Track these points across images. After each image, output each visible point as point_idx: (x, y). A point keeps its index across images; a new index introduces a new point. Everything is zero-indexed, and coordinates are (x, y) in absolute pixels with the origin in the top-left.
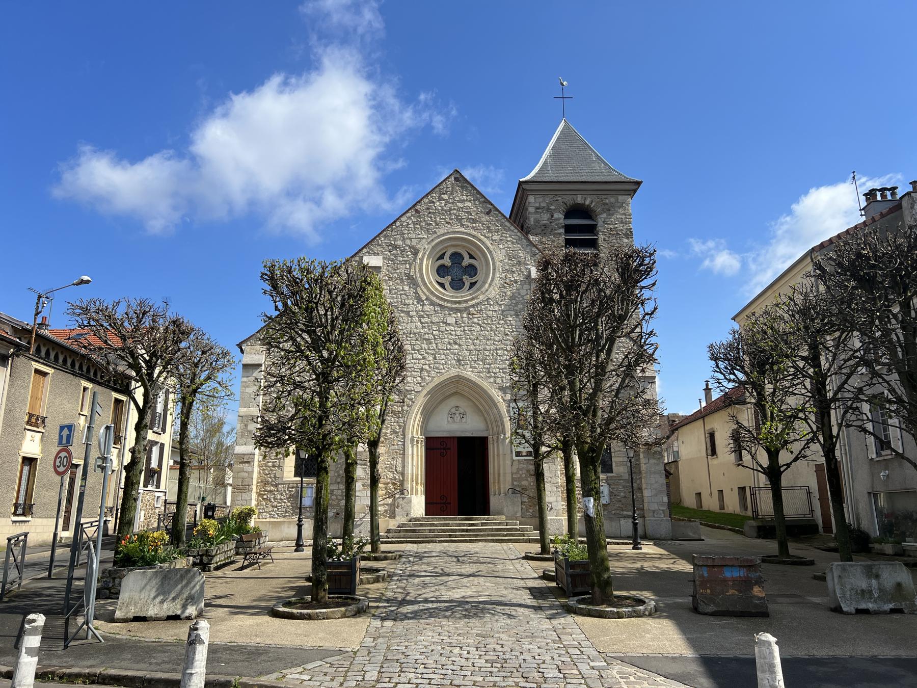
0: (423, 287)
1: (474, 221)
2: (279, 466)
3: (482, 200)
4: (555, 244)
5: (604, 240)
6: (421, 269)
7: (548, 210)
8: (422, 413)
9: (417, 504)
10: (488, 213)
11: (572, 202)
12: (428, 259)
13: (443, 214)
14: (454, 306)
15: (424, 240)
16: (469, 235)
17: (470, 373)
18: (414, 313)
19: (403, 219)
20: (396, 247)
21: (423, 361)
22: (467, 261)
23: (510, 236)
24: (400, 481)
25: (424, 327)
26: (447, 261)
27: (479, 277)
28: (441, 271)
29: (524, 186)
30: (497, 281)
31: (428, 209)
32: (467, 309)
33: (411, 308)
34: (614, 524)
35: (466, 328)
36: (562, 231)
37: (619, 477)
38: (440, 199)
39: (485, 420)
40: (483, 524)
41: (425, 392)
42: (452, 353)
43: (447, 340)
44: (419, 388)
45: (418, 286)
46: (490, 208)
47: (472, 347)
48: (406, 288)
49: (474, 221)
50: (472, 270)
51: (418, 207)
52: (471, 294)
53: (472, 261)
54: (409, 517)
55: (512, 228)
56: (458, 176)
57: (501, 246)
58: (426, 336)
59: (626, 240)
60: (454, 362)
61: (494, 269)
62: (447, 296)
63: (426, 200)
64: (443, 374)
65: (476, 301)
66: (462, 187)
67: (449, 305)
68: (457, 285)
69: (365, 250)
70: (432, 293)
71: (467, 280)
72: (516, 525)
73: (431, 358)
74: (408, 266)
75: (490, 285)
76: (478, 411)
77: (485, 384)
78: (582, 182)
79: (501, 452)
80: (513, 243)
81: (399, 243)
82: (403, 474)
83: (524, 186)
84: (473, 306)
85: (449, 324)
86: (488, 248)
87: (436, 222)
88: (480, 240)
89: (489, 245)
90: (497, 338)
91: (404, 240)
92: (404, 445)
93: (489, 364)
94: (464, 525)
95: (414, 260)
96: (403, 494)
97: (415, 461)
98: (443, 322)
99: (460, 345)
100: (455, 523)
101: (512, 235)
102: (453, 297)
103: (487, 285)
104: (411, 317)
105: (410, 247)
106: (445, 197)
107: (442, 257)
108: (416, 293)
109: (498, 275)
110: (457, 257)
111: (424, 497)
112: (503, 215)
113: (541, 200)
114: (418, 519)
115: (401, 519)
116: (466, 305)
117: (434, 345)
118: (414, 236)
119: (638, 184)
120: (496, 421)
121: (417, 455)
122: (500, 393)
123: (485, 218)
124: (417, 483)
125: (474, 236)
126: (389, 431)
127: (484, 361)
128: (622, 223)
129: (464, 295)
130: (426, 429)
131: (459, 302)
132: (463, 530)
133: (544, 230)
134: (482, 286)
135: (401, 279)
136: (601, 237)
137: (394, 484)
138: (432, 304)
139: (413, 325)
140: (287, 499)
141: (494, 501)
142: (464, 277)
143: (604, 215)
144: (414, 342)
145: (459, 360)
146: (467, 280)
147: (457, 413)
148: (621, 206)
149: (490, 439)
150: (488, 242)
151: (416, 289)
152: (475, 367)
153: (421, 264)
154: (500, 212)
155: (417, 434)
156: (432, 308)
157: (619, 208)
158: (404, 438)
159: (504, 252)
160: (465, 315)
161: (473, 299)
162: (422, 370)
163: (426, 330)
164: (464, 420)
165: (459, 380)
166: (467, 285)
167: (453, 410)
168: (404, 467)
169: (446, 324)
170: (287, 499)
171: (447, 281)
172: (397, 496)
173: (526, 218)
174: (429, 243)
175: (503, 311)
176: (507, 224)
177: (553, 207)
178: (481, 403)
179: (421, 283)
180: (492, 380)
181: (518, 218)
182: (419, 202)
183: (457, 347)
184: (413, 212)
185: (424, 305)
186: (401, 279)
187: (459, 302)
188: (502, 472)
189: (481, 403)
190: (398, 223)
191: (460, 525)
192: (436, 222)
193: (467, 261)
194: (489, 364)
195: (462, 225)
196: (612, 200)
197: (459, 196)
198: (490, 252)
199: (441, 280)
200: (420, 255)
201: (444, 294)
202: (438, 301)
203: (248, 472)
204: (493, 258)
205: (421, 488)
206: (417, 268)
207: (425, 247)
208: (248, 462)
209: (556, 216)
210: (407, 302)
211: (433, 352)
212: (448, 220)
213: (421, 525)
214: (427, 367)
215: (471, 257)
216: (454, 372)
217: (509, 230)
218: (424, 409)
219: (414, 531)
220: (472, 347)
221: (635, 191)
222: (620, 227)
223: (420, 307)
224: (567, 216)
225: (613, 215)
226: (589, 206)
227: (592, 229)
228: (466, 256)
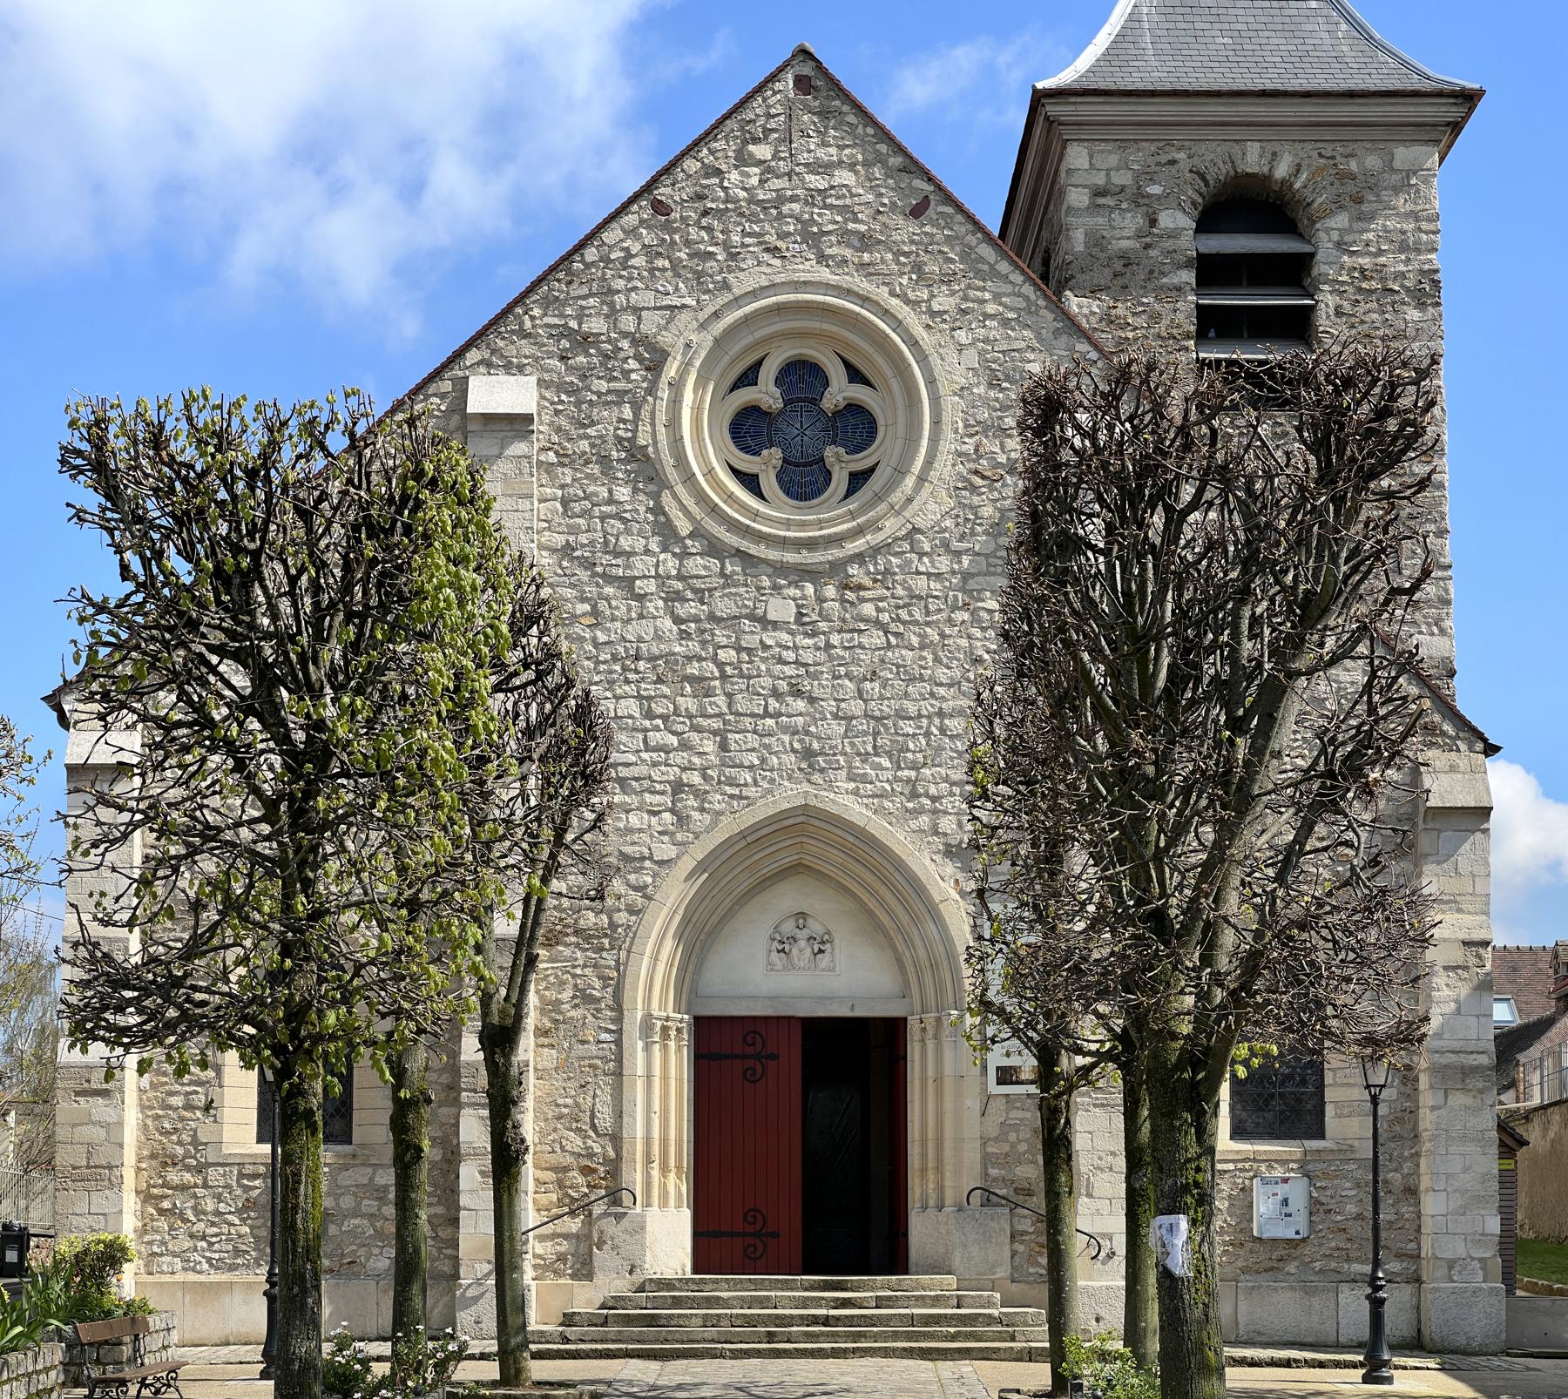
0: (680, 489)
1: (865, 242)
2: (208, 1107)
3: (896, 161)
4: (1162, 327)
5: (1339, 312)
6: (674, 424)
7: (1139, 199)
8: (679, 936)
9: (666, 1237)
10: (917, 212)
12: (701, 383)
13: (753, 218)
14: (791, 557)
15: (685, 316)
16: (848, 293)
17: (849, 800)
18: (650, 586)
19: (609, 237)
20: (585, 341)
21: (681, 758)
22: (839, 391)
23: (997, 297)
24: (606, 1161)
25: (684, 635)
26: (766, 393)
27: (882, 450)
28: (748, 429)
29: (1052, 109)
30: (945, 467)
31: (700, 197)
32: (837, 567)
33: (641, 565)
34: (1316, 1302)
35: (835, 639)
36: (1188, 276)
37: (1344, 1153)
38: (743, 160)
39: (899, 961)
40: (880, 1302)
41: (687, 864)
42: (785, 729)
43: (767, 682)
44: (665, 850)
45: (665, 484)
46: (927, 196)
47: (856, 707)
48: (623, 493)
49: (865, 242)
50: (857, 426)
51: (663, 192)
52: (853, 515)
53: (859, 393)
54: (638, 1278)
55: (1004, 267)
56: (807, 69)
57: (963, 336)
58: (693, 669)
59: (1413, 314)
60: (790, 760)
61: (936, 423)
62: (769, 520)
63: (691, 165)
64: (751, 802)
65: (871, 539)
66: (824, 114)
67: (773, 555)
68: (804, 481)
69: (473, 356)
70: (714, 510)
71: (840, 462)
72: (990, 1304)
73: (709, 746)
74: (627, 413)
75: (922, 479)
76: (875, 928)
77: (899, 839)
78: (1263, 93)
79: (948, 1070)
80: (1005, 323)
81: (596, 325)
82: (616, 1139)
83: (1052, 109)
84: (859, 558)
85: (775, 625)
86: (914, 344)
87: (727, 245)
88: (886, 314)
89: (919, 332)
90: (942, 674)
91: (613, 314)
92: (618, 1043)
93: (915, 767)
94: (817, 1303)
95: (652, 391)
96: (617, 1202)
97: (659, 1098)
98: (752, 617)
99: (812, 700)
100: (791, 1295)
101: (1007, 290)
102: (788, 524)
103: (910, 481)
104: (641, 598)
105: (635, 342)
106: (762, 151)
107: (748, 377)
108: (658, 510)
109: (948, 444)
110: (802, 377)
111: (686, 1215)
112: (970, 218)
113: (1113, 160)
114: (667, 1284)
115: (610, 1283)
116: (835, 553)
117: (721, 701)
118: (647, 299)
119: (1469, 98)
120: (934, 966)
121: (665, 1078)
122: (950, 868)
123: (905, 230)
124: (664, 1169)
125: (864, 300)
126: (567, 995)
127: (897, 755)
128: (1404, 247)
129: (829, 516)
130: (694, 990)
131: (811, 544)
132: (815, 1320)
133: (1123, 274)
134: (891, 486)
135: (604, 461)
136: (1327, 300)
137: (587, 1171)
138: (715, 549)
139: (645, 629)
140: (238, 1211)
141: (921, 1230)
142: (830, 452)
143: (1340, 220)
144: (648, 689)
145: (808, 754)
146: (840, 462)
148: (1402, 187)
149: (913, 1026)
150: (914, 322)
151: (656, 496)
152: (864, 779)
153: (676, 402)
154: (959, 208)
155: (663, 1005)
156: (714, 564)
157: (1397, 190)
158: (619, 1020)
159: (971, 357)
160: (830, 591)
161: (859, 532)
162: (678, 787)
163: (694, 646)
164: (824, 960)
165: (804, 823)
166: (840, 480)
167: (789, 927)
168: (619, 1115)
169: (765, 623)
170: (238, 1211)
171: (767, 464)
172: (598, 1210)
173: (1060, 230)
174: (703, 326)
175: (966, 576)
176: (986, 251)
177: (1155, 190)
178: (882, 903)
179: (672, 475)
180: (924, 821)
181: (1032, 234)
182: (667, 170)
183: (801, 705)
184: (643, 210)
185: (685, 554)
186: (604, 461)
187: (811, 544)
188: (948, 1133)
189: (882, 903)
190: (591, 254)
191: (805, 1303)
192: (727, 245)
193: (839, 391)
194: (915, 767)
195: (822, 258)
196: (1373, 162)
197: (812, 148)
198: (923, 359)
199: (747, 463)
200: (671, 370)
201: (756, 515)
202: (733, 540)
203: (106, 1126)
204: (931, 382)
205: (679, 1186)
206: (662, 418)
207: (689, 340)
208: (104, 1093)
209: (1167, 220)
210: (625, 543)
211: (716, 724)
212: (772, 239)
213: (677, 1302)
214: (696, 778)
215: (855, 375)
216: (789, 795)
217: (994, 274)
218: (686, 921)
219: (652, 1321)
220: (856, 707)
221: (1456, 127)
222: (1394, 263)
223: (670, 564)
224: (1207, 222)
225: (1372, 218)
226: (1286, 184)
227: (1295, 271)
228: (837, 374)
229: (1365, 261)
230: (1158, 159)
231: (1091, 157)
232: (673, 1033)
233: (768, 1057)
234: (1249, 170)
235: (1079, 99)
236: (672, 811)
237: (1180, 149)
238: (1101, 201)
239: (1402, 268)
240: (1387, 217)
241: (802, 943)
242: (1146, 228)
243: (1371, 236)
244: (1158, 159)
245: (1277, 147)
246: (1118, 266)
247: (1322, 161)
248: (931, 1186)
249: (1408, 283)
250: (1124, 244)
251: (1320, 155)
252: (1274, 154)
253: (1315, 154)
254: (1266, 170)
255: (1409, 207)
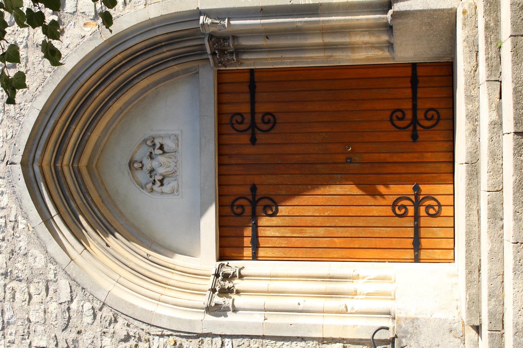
114: (474, 303)
147: (148, 164)
164: (169, 144)
232: (227, 284)
233: (254, 196)
236: (29, 281)
241: (155, 164)
248: (367, 39)
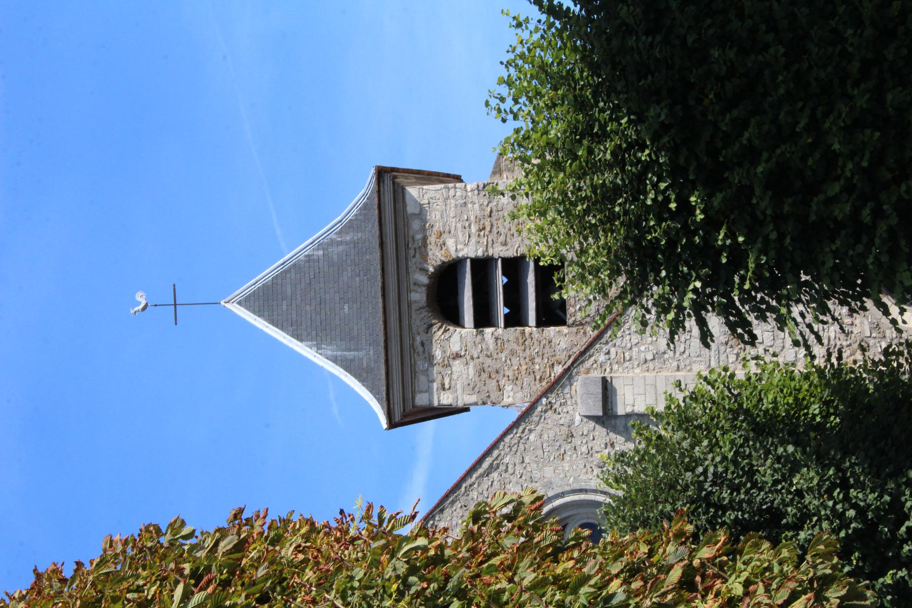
5: (505, 244)
11: (425, 313)
29: (397, 418)
36: (488, 331)
83: (397, 418)
136: (499, 251)
143: (450, 243)
209: (455, 346)
224: (456, 320)
226: (431, 277)
227: (482, 267)
229: (474, 229)
230: (421, 353)
231: (421, 392)
234: (425, 298)
235: (391, 402)
237: (414, 339)
238: (447, 386)
239: (477, 206)
240: (448, 216)
242: (463, 360)
243: (459, 225)
244: (421, 353)
245: (412, 283)
246: (484, 376)
247: (417, 255)
249: (486, 203)
250: (471, 371)
251: (414, 256)
252: (415, 284)
253: (414, 260)
254: (424, 289)
255: (440, 202)
